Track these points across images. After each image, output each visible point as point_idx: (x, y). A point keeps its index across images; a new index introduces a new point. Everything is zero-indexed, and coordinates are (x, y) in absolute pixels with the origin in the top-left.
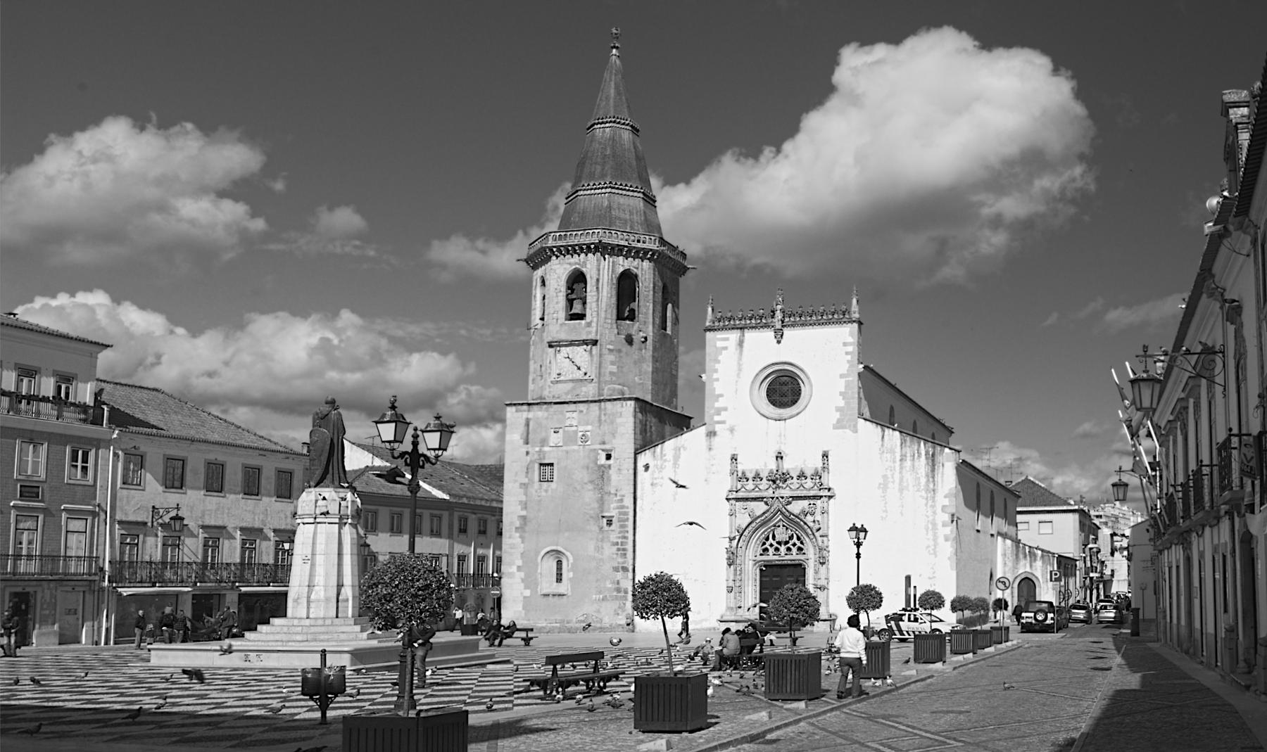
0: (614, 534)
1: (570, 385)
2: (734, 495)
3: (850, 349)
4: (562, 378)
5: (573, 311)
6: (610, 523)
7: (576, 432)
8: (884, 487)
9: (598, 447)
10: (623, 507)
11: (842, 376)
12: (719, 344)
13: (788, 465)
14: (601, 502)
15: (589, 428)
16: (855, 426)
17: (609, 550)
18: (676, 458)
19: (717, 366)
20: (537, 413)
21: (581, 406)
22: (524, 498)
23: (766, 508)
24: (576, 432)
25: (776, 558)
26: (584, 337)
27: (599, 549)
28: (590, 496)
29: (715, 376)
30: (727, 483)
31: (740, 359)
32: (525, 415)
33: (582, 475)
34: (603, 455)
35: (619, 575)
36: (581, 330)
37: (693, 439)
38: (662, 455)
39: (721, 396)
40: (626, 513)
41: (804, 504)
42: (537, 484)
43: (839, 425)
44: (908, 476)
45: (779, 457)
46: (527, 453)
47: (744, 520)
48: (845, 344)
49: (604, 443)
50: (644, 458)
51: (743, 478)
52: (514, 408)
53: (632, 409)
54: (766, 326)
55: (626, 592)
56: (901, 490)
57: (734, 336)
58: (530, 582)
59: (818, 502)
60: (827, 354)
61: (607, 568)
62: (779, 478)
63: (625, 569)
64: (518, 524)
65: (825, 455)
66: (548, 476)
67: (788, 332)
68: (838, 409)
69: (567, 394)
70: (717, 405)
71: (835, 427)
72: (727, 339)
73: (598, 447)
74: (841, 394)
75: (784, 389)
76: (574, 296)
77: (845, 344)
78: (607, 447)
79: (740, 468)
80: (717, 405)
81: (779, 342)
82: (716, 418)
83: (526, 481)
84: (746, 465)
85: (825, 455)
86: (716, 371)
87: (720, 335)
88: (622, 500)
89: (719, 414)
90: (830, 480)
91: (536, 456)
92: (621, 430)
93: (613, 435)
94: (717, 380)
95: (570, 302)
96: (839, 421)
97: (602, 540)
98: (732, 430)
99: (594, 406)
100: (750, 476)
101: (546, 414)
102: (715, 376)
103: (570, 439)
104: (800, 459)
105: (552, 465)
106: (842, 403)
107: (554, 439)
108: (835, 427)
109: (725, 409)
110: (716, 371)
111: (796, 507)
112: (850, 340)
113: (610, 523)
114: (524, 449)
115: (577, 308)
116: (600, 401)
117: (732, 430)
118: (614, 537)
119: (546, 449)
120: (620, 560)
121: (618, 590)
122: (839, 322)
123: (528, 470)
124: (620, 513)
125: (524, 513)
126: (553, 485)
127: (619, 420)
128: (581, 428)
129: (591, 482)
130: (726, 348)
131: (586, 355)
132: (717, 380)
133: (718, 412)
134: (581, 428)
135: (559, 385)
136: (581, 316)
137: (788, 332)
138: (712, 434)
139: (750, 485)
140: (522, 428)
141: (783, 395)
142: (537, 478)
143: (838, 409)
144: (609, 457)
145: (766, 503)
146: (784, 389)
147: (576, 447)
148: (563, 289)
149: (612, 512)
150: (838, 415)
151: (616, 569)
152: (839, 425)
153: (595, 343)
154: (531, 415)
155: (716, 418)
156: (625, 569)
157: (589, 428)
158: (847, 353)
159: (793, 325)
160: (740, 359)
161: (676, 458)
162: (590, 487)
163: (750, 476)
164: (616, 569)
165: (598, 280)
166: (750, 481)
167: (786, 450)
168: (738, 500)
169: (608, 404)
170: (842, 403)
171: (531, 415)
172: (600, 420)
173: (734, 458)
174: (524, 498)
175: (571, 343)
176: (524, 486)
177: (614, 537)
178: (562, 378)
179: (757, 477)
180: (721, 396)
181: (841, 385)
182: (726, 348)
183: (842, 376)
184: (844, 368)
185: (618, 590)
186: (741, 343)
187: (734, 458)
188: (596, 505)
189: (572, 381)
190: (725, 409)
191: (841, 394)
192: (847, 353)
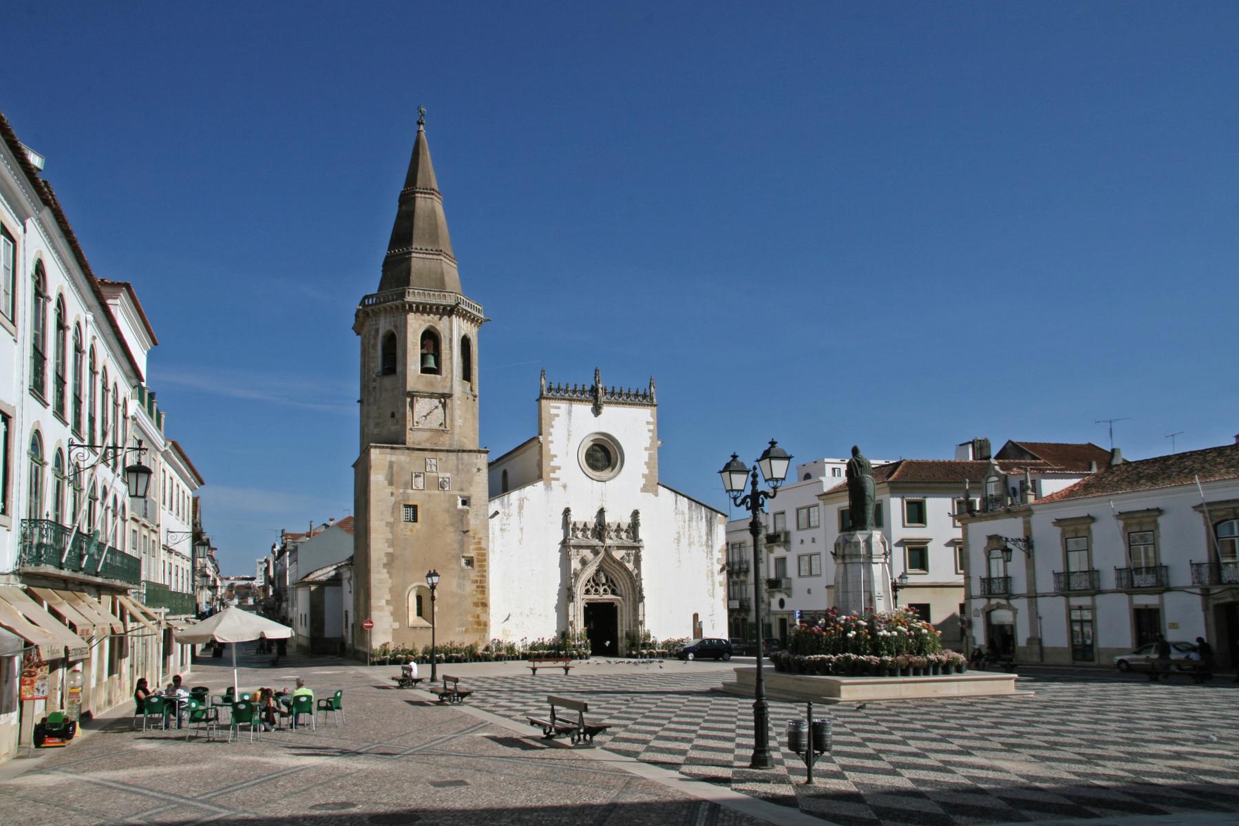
0: (473, 574)
1: (427, 435)
3: (651, 427)
8: (678, 540)
9: (457, 493)
10: (481, 549)
11: (646, 449)
12: (553, 411)
13: (609, 519)
14: (462, 545)
15: (448, 475)
17: (470, 588)
18: (521, 507)
20: (400, 457)
21: (441, 455)
22: (390, 536)
26: (440, 391)
27: (460, 586)
28: (451, 537)
29: (550, 438)
31: (569, 425)
32: (389, 458)
33: (444, 518)
34: (460, 502)
35: (479, 610)
36: (437, 383)
37: (533, 492)
38: (509, 505)
40: (484, 555)
41: (623, 553)
42: (402, 525)
43: (645, 489)
44: (695, 534)
46: (392, 494)
48: (648, 423)
49: (462, 490)
50: (495, 505)
55: (486, 625)
56: (690, 545)
57: (564, 406)
58: (399, 614)
60: (632, 426)
61: (468, 603)
64: (385, 560)
65: (636, 514)
67: (606, 410)
68: (644, 476)
69: (427, 441)
70: (552, 464)
73: (457, 493)
76: (425, 351)
77: (648, 423)
78: (466, 494)
79: (573, 518)
80: (552, 464)
82: (552, 475)
83: (391, 520)
85: (636, 514)
86: (551, 434)
87: (553, 403)
88: (479, 543)
90: (642, 534)
91: (400, 498)
93: (470, 483)
96: (645, 486)
97: (464, 578)
98: (565, 487)
99: (452, 456)
100: (581, 526)
101: (408, 459)
102: (550, 438)
104: (617, 516)
106: (646, 472)
110: (551, 434)
111: (618, 554)
112: (651, 420)
113: (470, 562)
114: (389, 490)
115: (431, 363)
117: (565, 487)
119: (410, 491)
121: (479, 623)
122: (641, 405)
123: (394, 509)
125: (391, 550)
126: (417, 525)
128: (441, 475)
129: (452, 525)
130: (558, 415)
133: (554, 469)
135: (419, 433)
138: (548, 487)
140: (386, 470)
141: (597, 460)
142: (403, 517)
143: (644, 476)
144: (464, 503)
149: (472, 554)
150: (643, 481)
151: (476, 605)
152: (645, 489)
154: (394, 458)
155: (552, 475)
157: (448, 475)
160: (569, 425)
161: (521, 507)
162: (451, 529)
164: (476, 605)
165: (451, 340)
167: (606, 508)
168: (575, 547)
170: (646, 472)
171: (394, 458)
172: (458, 469)
173: (567, 512)
174: (390, 536)
175: (431, 396)
181: (645, 456)
182: (558, 415)
183: (646, 449)
184: (647, 443)
185: (479, 623)
186: (570, 413)
187: (567, 512)
188: (456, 546)
189: (431, 430)
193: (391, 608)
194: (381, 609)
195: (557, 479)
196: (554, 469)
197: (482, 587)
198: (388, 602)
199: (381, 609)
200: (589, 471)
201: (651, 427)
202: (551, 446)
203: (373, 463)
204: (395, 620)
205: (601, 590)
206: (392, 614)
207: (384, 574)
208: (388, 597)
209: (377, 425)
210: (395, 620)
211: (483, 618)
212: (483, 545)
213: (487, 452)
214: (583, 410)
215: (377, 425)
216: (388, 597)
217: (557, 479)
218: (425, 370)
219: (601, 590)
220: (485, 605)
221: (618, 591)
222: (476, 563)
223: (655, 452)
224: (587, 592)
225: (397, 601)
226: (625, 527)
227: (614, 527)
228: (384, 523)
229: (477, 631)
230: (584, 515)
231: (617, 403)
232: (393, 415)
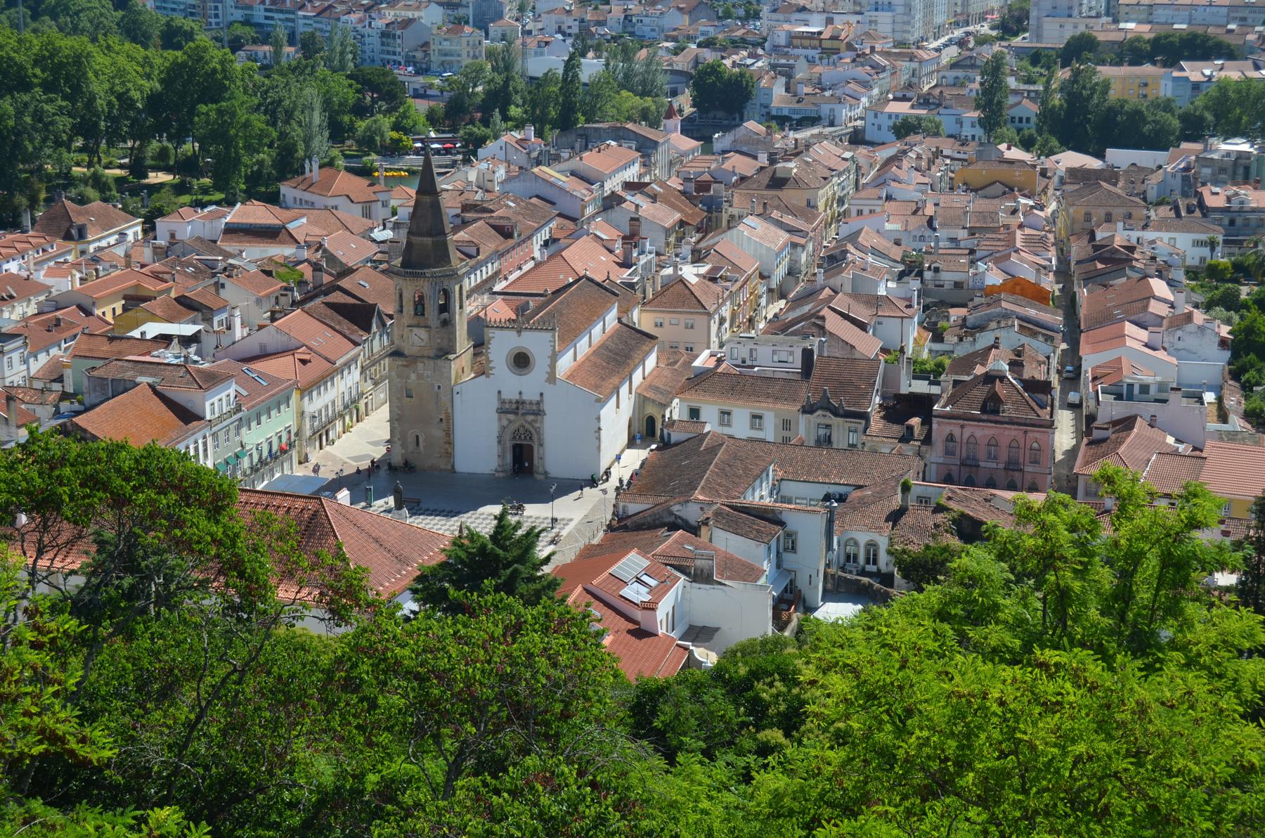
0: (444, 425)
13: (525, 397)
30: (495, 404)
51: (503, 402)
84: (504, 396)
103: (420, 377)
107: (413, 376)
133: (491, 369)
149: (443, 417)
179: (511, 402)
214: (510, 335)
220: (450, 443)
224: (514, 438)
230: (510, 394)
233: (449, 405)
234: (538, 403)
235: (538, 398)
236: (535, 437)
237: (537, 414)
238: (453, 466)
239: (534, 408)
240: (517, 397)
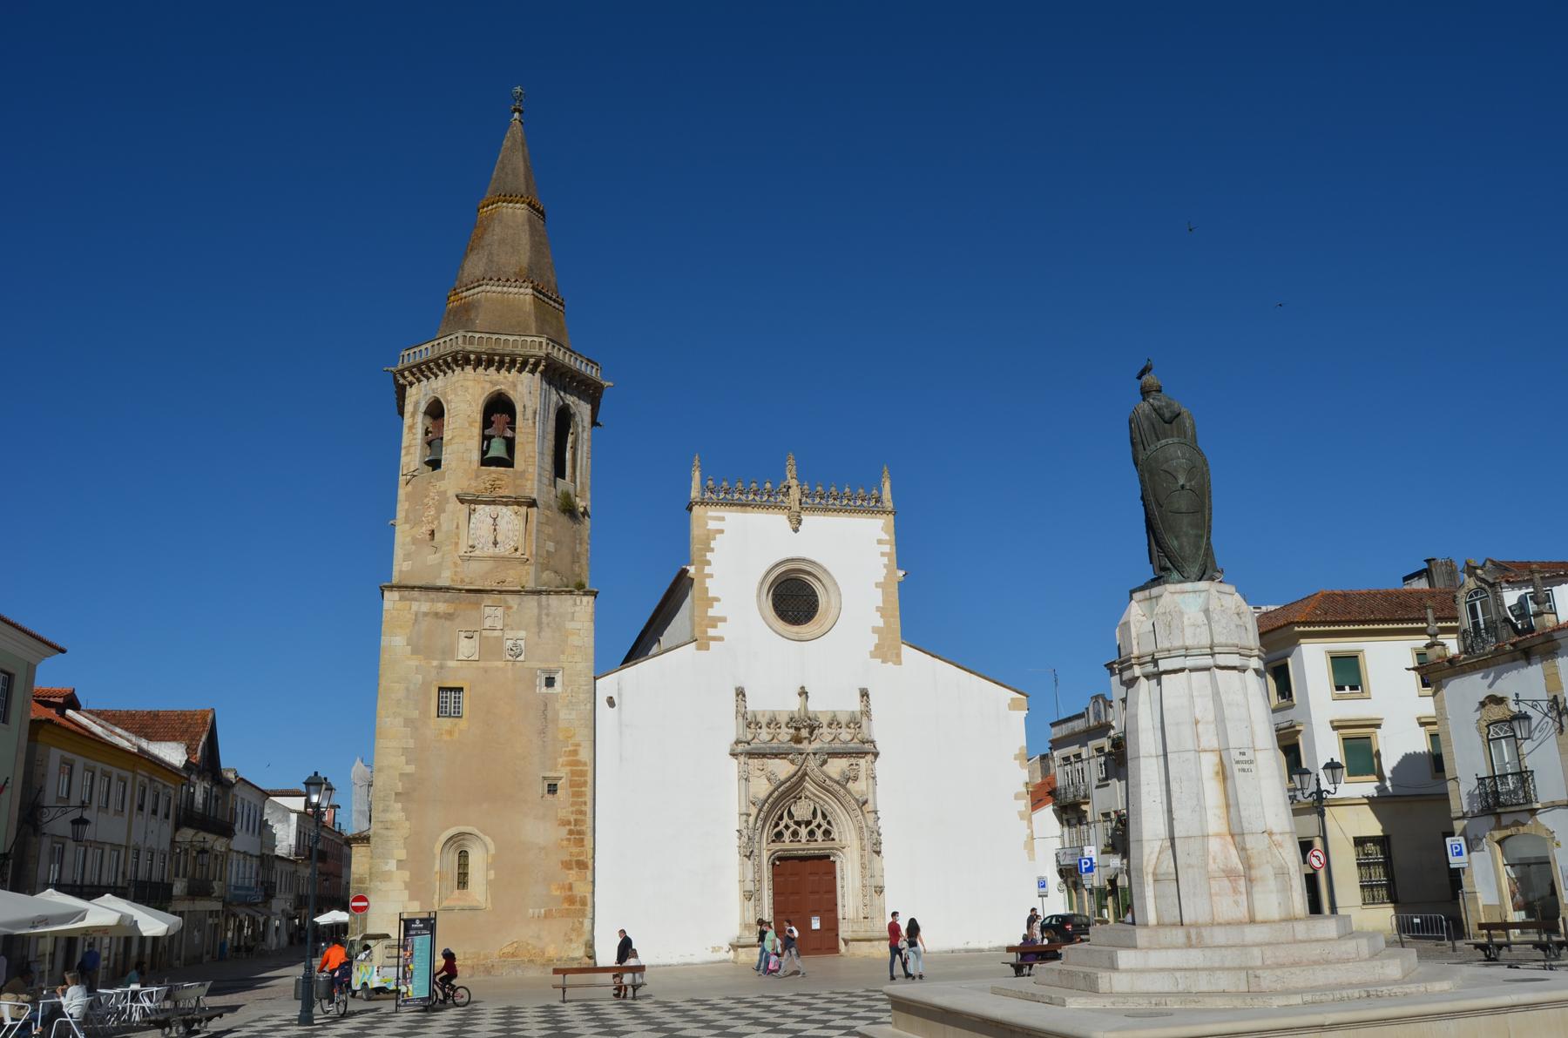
1: (491, 564)
2: (740, 748)
4: (477, 553)
5: (491, 454)
6: (552, 789)
7: (499, 640)
10: (577, 763)
11: (877, 585)
12: (712, 525)
13: (814, 706)
16: (898, 655)
19: (709, 556)
21: (509, 597)
22: (411, 743)
23: (792, 769)
24: (499, 640)
25: (796, 845)
29: (707, 570)
30: (730, 729)
35: (572, 875)
39: (717, 600)
40: (583, 774)
45: (803, 693)
47: (762, 788)
48: (880, 542)
50: (606, 686)
51: (751, 723)
52: (396, 595)
53: (590, 609)
54: (777, 507)
55: (584, 903)
59: (862, 762)
62: (804, 726)
63: (582, 865)
65: (864, 694)
66: (451, 706)
68: (875, 630)
70: (711, 612)
71: (873, 655)
72: (722, 519)
74: (878, 609)
75: (794, 598)
77: (880, 542)
80: (711, 612)
81: (796, 530)
82: (711, 632)
85: (864, 694)
86: (708, 563)
87: (713, 512)
88: (575, 752)
89: (715, 627)
92: (574, 640)
94: (711, 576)
95: (486, 438)
96: (877, 646)
99: (531, 601)
100: (764, 721)
103: (490, 649)
104: (832, 700)
105: (461, 689)
107: (466, 648)
108: (873, 655)
109: (724, 620)
110: (708, 563)
112: (886, 537)
115: (498, 449)
116: (539, 593)
118: (566, 812)
119: (451, 664)
120: (575, 850)
124: (573, 773)
125: (410, 769)
127: (570, 625)
130: (721, 532)
131: (519, 523)
132: (711, 576)
133: (714, 622)
134: (509, 634)
135: (474, 565)
136: (507, 462)
137: (808, 520)
139: (764, 735)
143: (875, 630)
145: (792, 762)
146: (794, 598)
147: (500, 664)
148: (479, 418)
149: (562, 773)
150: (875, 639)
151: (567, 865)
153: (532, 504)
155: (711, 632)
156: (582, 865)
157: (522, 634)
158: (883, 554)
159: (813, 509)
163: (764, 721)
164: (567, 865)
166: (764, 729)
169: (553, 599)
170: (880, 623)
172: (539, 623)
173: (740, 693)
176: (408, 722)
177: (566, 812)
178: (477, 553)
179: (773, 722)
180: (717, 600)
181: (877, 598)
182: (721, 532)
183: (877, 585)
184: (881, 574)
187: (740, 693)
190: (724, 620)
191: (878, 609)
192: (883, 554)
193: (406, 875)
194: (386, 876)
195: (721, 639)
196: (714, 622)
197: (580, 832)
198: (401, 864)
199: (386, 876)
200: (780, 625)
201: (887, 548)
202: (708, 582)
203: (386, 616)
204: (412, 898)
205: (803, 831)
206: (407, 886)
207: (396, 813)
208: (401, 854)
209: (407, 557)
210: (412, 898)
211: (581, 889)
212: (584, 755)
213: (595, 594)
215: (407, 557)
216: (401, 854)
217: (721, 639)
218: (486, 461)
219: (803, 831)
220: (584, 865)
221: (835, 835)
222: (571, 789)
223: (894, 590)
225: (416, 863)
226: (843, 719)
227: (825, 721)
228: (399, 721)
229: (566, 914)
230: (774, 698)
231: (826, 510)
232: (432, 533)
233: (582, 735)
234: (855, 722)
235: (856, 705)
236: (846, 833)
237: (861, 754)
238: (590, 945)
239: (845, 735)
240: (794, 705)
